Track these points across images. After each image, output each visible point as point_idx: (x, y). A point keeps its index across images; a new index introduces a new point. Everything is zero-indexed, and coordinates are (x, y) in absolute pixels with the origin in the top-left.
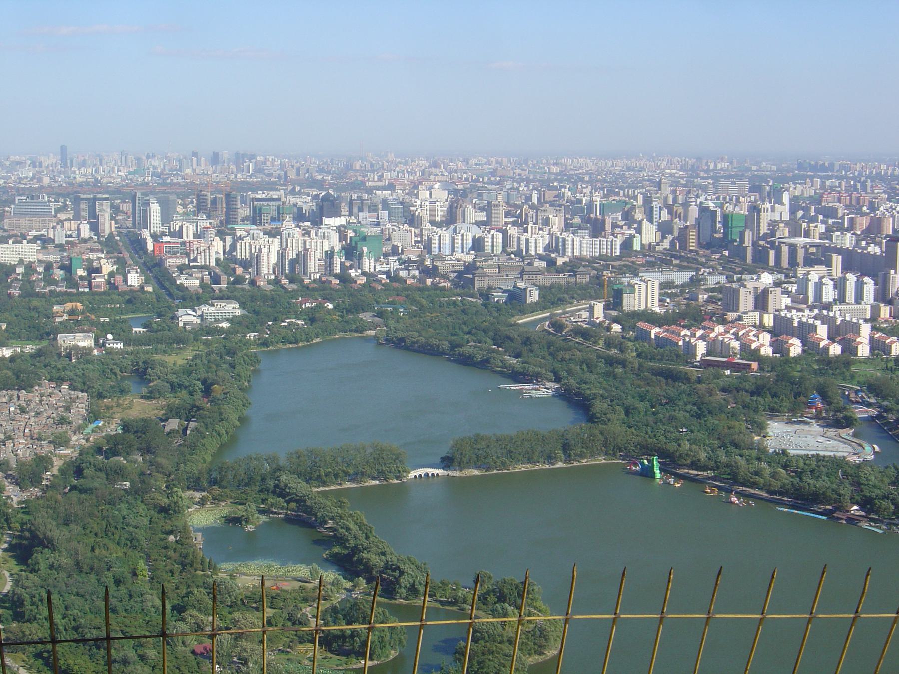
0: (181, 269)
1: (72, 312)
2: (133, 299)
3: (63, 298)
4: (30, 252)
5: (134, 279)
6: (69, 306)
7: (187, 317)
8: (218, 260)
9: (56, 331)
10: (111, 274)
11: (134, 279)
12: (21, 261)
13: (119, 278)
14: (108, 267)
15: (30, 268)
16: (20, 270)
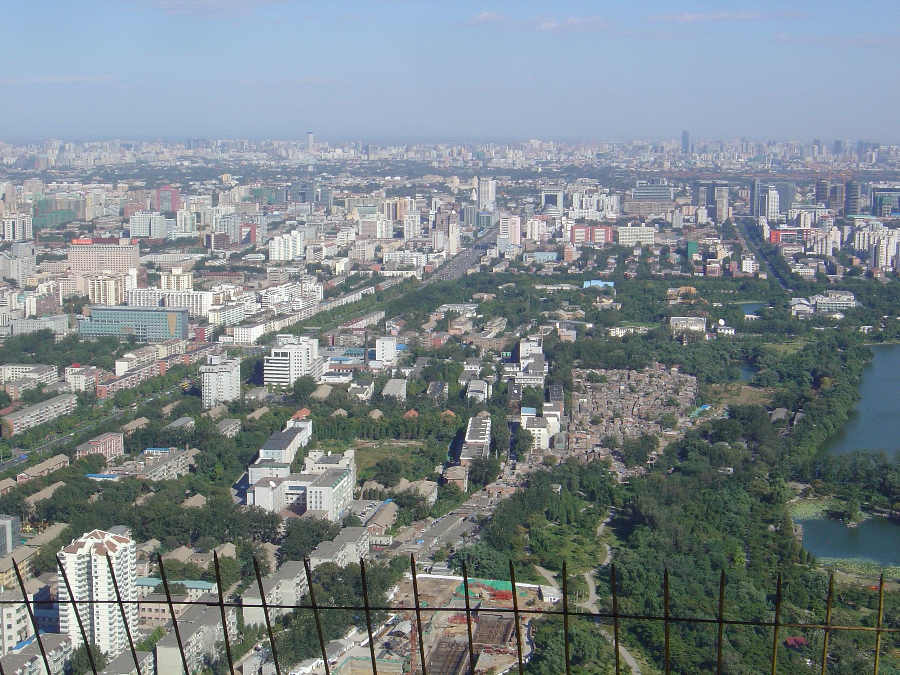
0: (797, 258)
1: (686, 296)
2: (747, 285)
3: (676, 282)
4: (648, 235)
5: (749, 266)
6: (683, 290)
7: (800, 307)
8: (835, 250)
9: (668, 314)
10: (726, 260)
11: (749, 266)
12: (639, 244)
13: (734, 265)
14: (723, 253)
15: (647, 251)
16: (637, 253)
